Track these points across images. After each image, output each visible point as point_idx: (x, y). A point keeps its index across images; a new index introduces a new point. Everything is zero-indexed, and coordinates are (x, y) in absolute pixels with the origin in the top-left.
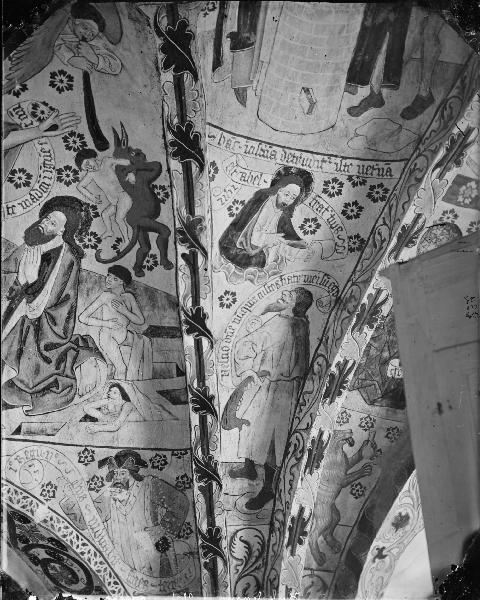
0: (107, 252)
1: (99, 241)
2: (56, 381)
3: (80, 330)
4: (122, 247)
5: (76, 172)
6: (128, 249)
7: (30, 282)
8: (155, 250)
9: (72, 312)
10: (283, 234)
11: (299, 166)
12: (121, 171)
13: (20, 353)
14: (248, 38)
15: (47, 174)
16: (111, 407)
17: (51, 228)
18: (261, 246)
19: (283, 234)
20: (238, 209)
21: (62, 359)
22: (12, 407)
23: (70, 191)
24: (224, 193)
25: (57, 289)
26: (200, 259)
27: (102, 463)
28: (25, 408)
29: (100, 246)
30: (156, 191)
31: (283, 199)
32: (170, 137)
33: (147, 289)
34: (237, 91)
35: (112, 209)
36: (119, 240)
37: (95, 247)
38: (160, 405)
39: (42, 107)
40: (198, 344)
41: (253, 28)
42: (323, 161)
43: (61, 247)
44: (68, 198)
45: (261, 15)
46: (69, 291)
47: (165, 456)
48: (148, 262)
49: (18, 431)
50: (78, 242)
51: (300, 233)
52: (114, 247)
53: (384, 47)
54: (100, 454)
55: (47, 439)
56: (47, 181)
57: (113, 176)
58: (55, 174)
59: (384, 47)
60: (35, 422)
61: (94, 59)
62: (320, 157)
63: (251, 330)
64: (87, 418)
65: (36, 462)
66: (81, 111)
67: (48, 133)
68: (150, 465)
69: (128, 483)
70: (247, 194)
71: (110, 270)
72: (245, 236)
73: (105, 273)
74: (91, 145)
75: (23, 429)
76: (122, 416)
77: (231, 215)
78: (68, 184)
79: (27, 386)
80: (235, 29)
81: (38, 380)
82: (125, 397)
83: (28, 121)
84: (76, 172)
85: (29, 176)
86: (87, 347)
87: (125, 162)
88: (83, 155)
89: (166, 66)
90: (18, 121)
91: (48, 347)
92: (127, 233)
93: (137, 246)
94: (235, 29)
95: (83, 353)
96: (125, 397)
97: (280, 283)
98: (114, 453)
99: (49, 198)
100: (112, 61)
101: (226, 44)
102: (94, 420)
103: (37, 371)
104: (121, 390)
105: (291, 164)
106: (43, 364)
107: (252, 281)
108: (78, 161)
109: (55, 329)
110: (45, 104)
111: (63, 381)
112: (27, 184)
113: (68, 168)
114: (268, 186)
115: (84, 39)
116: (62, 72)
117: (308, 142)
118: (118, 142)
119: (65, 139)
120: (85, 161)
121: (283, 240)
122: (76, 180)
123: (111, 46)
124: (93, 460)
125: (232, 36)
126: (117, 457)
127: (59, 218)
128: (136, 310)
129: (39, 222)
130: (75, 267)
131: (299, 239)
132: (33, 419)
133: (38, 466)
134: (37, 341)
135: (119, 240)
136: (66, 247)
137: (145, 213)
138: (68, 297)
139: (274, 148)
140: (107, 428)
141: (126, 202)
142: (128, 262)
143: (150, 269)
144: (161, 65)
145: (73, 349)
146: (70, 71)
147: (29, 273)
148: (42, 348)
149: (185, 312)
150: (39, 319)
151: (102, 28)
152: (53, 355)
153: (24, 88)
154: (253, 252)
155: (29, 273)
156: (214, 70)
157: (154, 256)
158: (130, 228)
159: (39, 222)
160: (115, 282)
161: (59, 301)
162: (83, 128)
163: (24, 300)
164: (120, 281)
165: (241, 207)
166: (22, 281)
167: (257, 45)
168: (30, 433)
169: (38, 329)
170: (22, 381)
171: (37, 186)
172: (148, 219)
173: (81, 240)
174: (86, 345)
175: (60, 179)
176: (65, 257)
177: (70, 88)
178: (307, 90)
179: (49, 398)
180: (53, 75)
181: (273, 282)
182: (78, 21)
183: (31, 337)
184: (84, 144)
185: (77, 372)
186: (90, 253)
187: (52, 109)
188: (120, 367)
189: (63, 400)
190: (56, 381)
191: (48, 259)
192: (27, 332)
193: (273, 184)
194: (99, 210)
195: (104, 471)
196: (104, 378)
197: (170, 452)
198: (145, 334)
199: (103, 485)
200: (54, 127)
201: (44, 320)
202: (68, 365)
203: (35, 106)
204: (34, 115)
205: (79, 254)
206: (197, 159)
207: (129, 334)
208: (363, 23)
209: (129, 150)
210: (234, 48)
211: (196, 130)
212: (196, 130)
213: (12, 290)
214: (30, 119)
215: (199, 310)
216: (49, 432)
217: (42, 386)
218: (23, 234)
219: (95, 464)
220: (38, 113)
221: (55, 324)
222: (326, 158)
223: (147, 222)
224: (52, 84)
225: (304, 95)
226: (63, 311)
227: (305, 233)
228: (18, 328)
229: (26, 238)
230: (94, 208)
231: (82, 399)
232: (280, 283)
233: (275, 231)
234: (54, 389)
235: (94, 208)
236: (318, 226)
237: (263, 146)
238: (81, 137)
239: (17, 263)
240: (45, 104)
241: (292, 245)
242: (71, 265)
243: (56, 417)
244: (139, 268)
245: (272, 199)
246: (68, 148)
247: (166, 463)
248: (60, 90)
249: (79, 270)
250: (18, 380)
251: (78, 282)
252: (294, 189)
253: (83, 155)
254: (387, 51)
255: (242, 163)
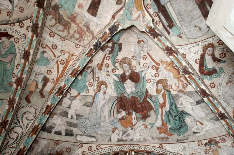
0: (175, 88)
1: (171, 86)
2: (181, 125)
3: (180, 110)
4: (177, 85)
5: (158, 74)
6: (179, 84)
7: (163, 102)
8: (185, 82)
9: (176, 105)
10: (216, 62)
11: (207, 43)
12: (166, 68)
13: (169, 120)
14: (173, 24)
15: (153, 77)
16: (199, 127)
17: (160, 88)
18: (212, 68)
19: (216, 62)
20: (198, 61)
21: (180, 118)
22: (174, 134)
23: (159, 78)
24: (191, 59)
25: (169, 103)
26: (193, 76)
27: (206, 145)
28: (177, 134)
29: (172, 87)
30: (175, 67)
31: (209, 53)
32: (166, 52)
33: (189, 92)
34: (178, 36)
35: (170, 77)
36: (176, 84)
37: (171, 88)
38: (213, 123)
39: (145, 64)
40: (209, 99)
41: (172, 22)
42: (213, 38)
43: (165, 92)
44: (160, 80)
45: (172, 19)
46: (172, 101)
47: (223, 138)
48: (185, 85)
49: (178, 140)
50: (167, 89)
51: (221, 59)
52: (176, 86)
53: (207, 5)
54: (204, 142)
55: (186, 141)
56: (154, 79)
57: (165, 70)
58: (154, 76)
59: (207, 5)
60: (181, 137)
61: (147, 49)
62: (212, 38)
63: (226, 91)
64: (194, 133)
65: (186, 148)
66: (152, 61)
67: (149, 69)
68: (220, 142)
69: (217, 149)
70: (198, 57)
71: (179, 91)
72: (206, 67)
73: (178, 93)
74: (157, 66)
75: (179, 139)
76: (204, 130)
77: (197, 64)
78: (158, 77)
79: (175, 128)
80: (168, 24)
81: (177, 126)
82: (201, 124)
83: (144, 69)
84: (158, 74)
85: (150, 79)
86: (184, 114)
87: (165, 65)
88: (157, 69)
89: (154, 38)
90: (142, 70)
91: (175, 116)
92: (176, 81)
93: (180, 83)
94: (168, 24)
95: (184, 115)
96: (201, 124)
97: (225, 74)
98: (207, 141)
99: (156, 82)
100: (149, 47)
101: (168, 28)
102: (196, 133)
103: (175, 124)
104: (199, 122)
105: (205, 44)
106: (176, 121)
107: (216, 77)
108: (157, 71)
109: (174, 111)
110: (145, 64)
111: (183, 124)
112: (151, 81)
113: (156, 74)
114: (202, 52)
115: (143, 47)
116: (144, 56)
117: (205, 37)
118: (161, 62)
119: (152, 68)
120: (158, 70)
121: (218, 63)
122: (159, 75)
123: (147, 44)
124: (202, 144)
125: (168, 26)
126: (209, 142)
127: (160, 85)
128: (190, 99)
129: (157, 88)
130: (170, 95)
131: (222, 60)
132: (181, 136)
133: (187, 149)
134: (172, 116)
135: (176, 84)
136: (166, 92)
137: (177, 74)
138: (172, 102)
139: (198, 43)
140: (201, 134)
141: (171, 74)
142: (181, 88)
143: (187, 87)
144: (153, 39)
145: (181, 115)
146: (144, 54)
147: (161, 101)
148: (173, 117)
149: (199, 92)
150: (169, 111)
151: (144, 42)
152: (177, 118)
153: (140, 63)
154: (211, 70)
155: (161, 101)
156: (169, 35)
157: (185, 83)
158: (176, 80)
159: (157, 88)
160: (180, 94)
161: (171, 104)
162: (154, 64)
163: (164, 107)
164: (182, 93)
165: (199, 61)
166: (161, 103)
167: (176, 24)
168: (181, 140)
169: (170, 113)
170: (173, 127)
171: (153, 81)
172: (178, 75)
173: (168, 88)
174: (183, 114)
175: (156, 77)
176: (167, 93)
177: (147, 58)
178: (196, 26)
179: (182, 130)
180: (143, 57)
181: (223, 75)
182: (140, 44)
183: (170, 116)
184: (156, 67)
185: (185, 121)
186: (171, 90)
187: (146, 64)
188: (195, 115)
189: (186, 129)
190: (181, 125)
191: (164, 96)
192: (168, 115)
193: (203, 51)
194: (167, 79)
195: (208, 147)
196: (193, 120)
197: (225, 136)
198: (196, 104)
199: (209, 152)
200: (149, 67)
201: (170, 110)
202: (182, 120)
203: (143, 65)
204: (144, 67)
205: (170, 92)
206: (175, 53)
207: (193, 106)
208: (197, 4)
209: (164, 62)
210: (170, 28)
211: (169, 47)
212: (169, 47)
213: (160, 106)
214: (144, 68)
215: (202, 89)
216: (186, 139)
217: (178, 127)
218: (156, 93)
219: (204, 145)
220: (145, 66)
221: (174, 110)
222: (213, 37)
223: (179, 76)
224: (144, 59)
225: (196, 27)
226: (173, 107)
227: (222, 58)
228: (166, 115)
229: (157, 93)
230: (166, 79)
231: (190, 128)
232: (225, 74)
233: (213, 62)
234: (182, 127)
235: (166, 79)
236: (225, 54)
237: (194, 44)
238: (154, 66)
239: (158, 99)
240: (145, 64)
241: (221, 63)
242: (169, 95)
243: (186, 134)
244: (184, 88)
245: (206, 54)
246: (153, 69)
247: (225, 140)
248: (146, 59)
249: (172, 95)
250: (172, 127)
251: (173, 98)
252: (210, 49)
253: (157, 69)
254: (208, 5)
255: (191, 50)
